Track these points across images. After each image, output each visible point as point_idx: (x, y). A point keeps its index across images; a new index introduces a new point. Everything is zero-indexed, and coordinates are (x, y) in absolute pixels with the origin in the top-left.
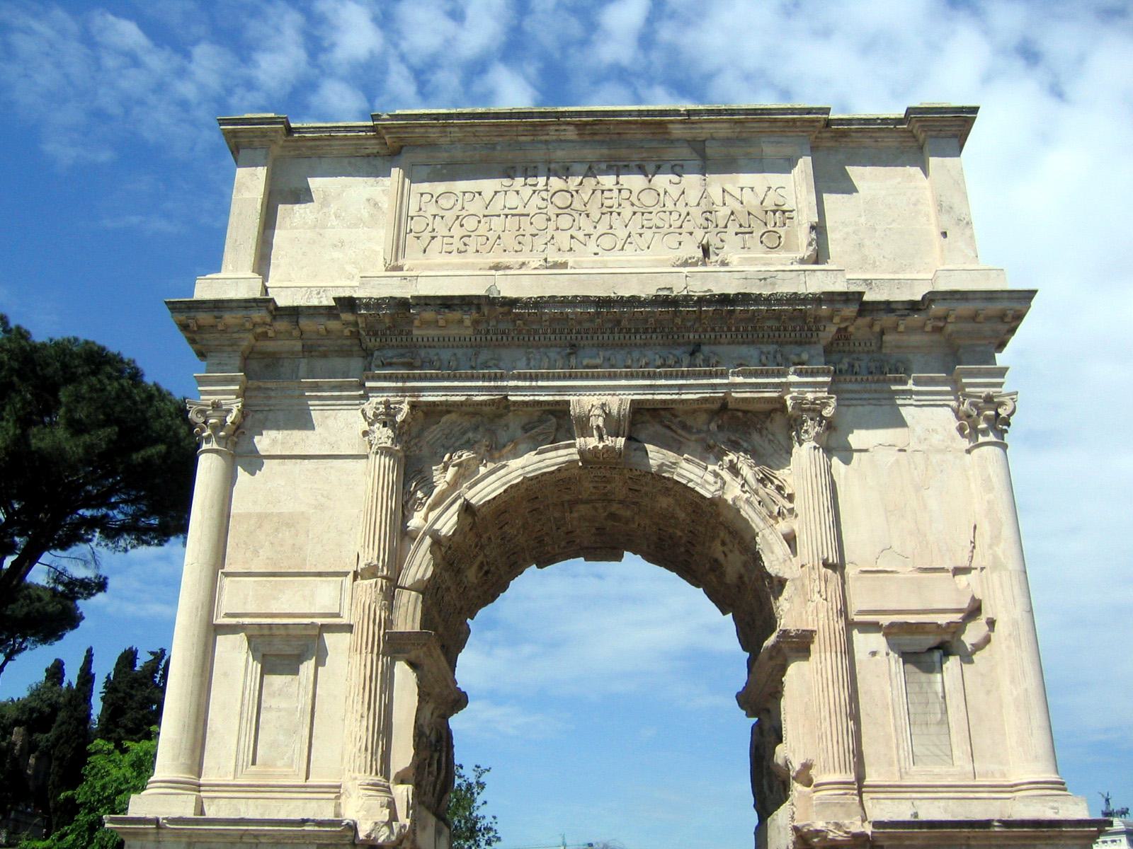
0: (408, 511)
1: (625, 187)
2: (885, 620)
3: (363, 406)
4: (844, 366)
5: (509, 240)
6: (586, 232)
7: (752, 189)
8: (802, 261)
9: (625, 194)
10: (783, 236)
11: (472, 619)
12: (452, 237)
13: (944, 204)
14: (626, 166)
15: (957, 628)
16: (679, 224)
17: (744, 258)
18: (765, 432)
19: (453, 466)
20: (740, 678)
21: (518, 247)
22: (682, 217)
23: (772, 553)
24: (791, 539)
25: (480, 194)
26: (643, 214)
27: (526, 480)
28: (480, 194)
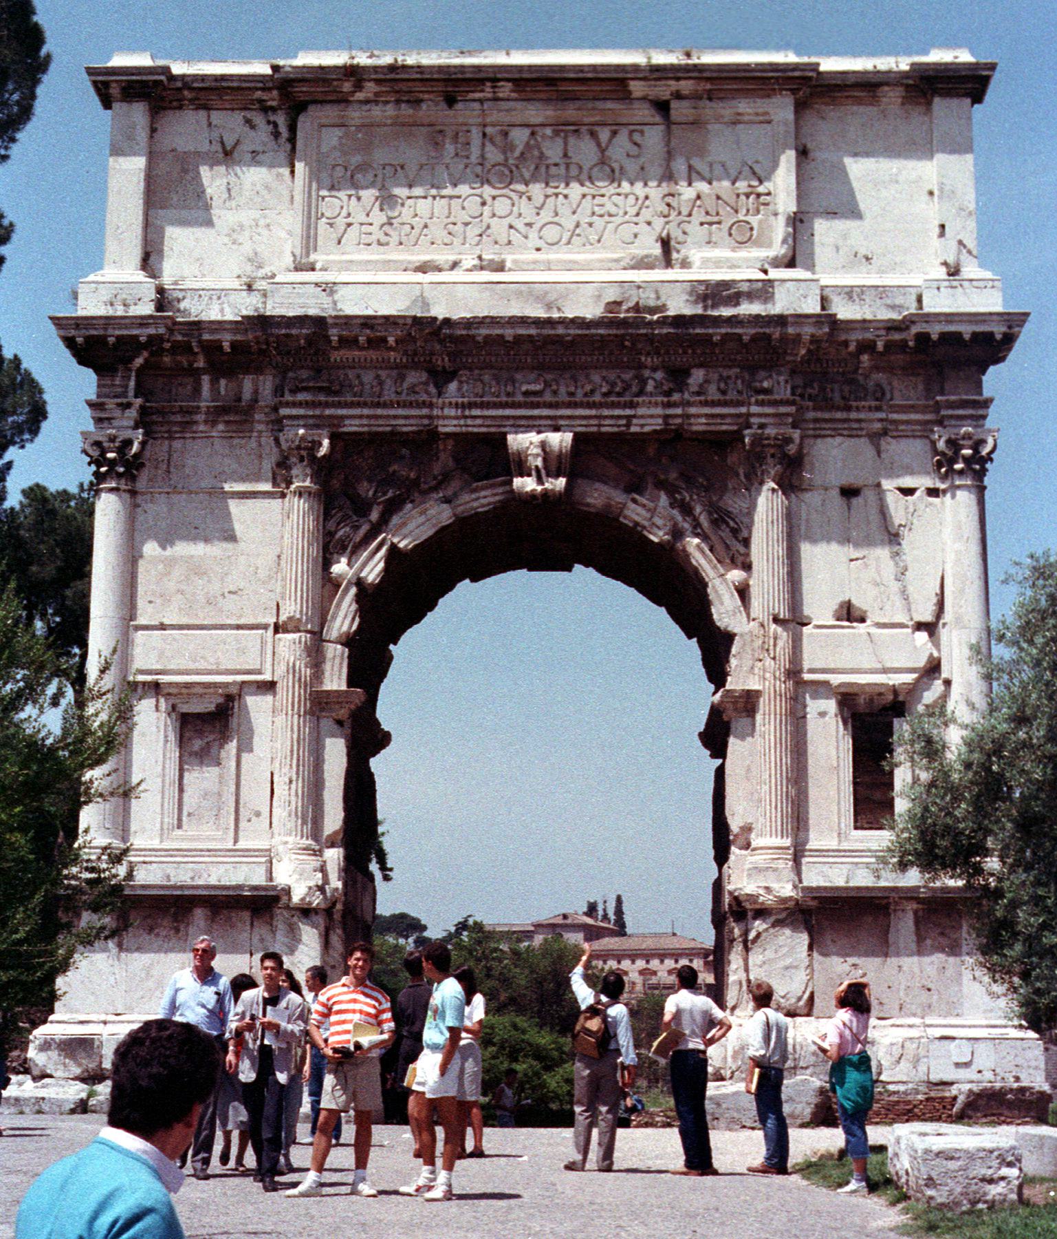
0: (331, 554)
2: (836, 679)
5: (437, 232)
6: (527, 221)
10: (755, 225)
11: (395, 644)
13: (947, 188)
14: (576, 131)
15: (914, 690)
16: (636, 209)
22: (640, 202)
23: (722, 604)
24: (743, 592)
25: (402, 167)
26: (594, 197)
28: (402, 167)
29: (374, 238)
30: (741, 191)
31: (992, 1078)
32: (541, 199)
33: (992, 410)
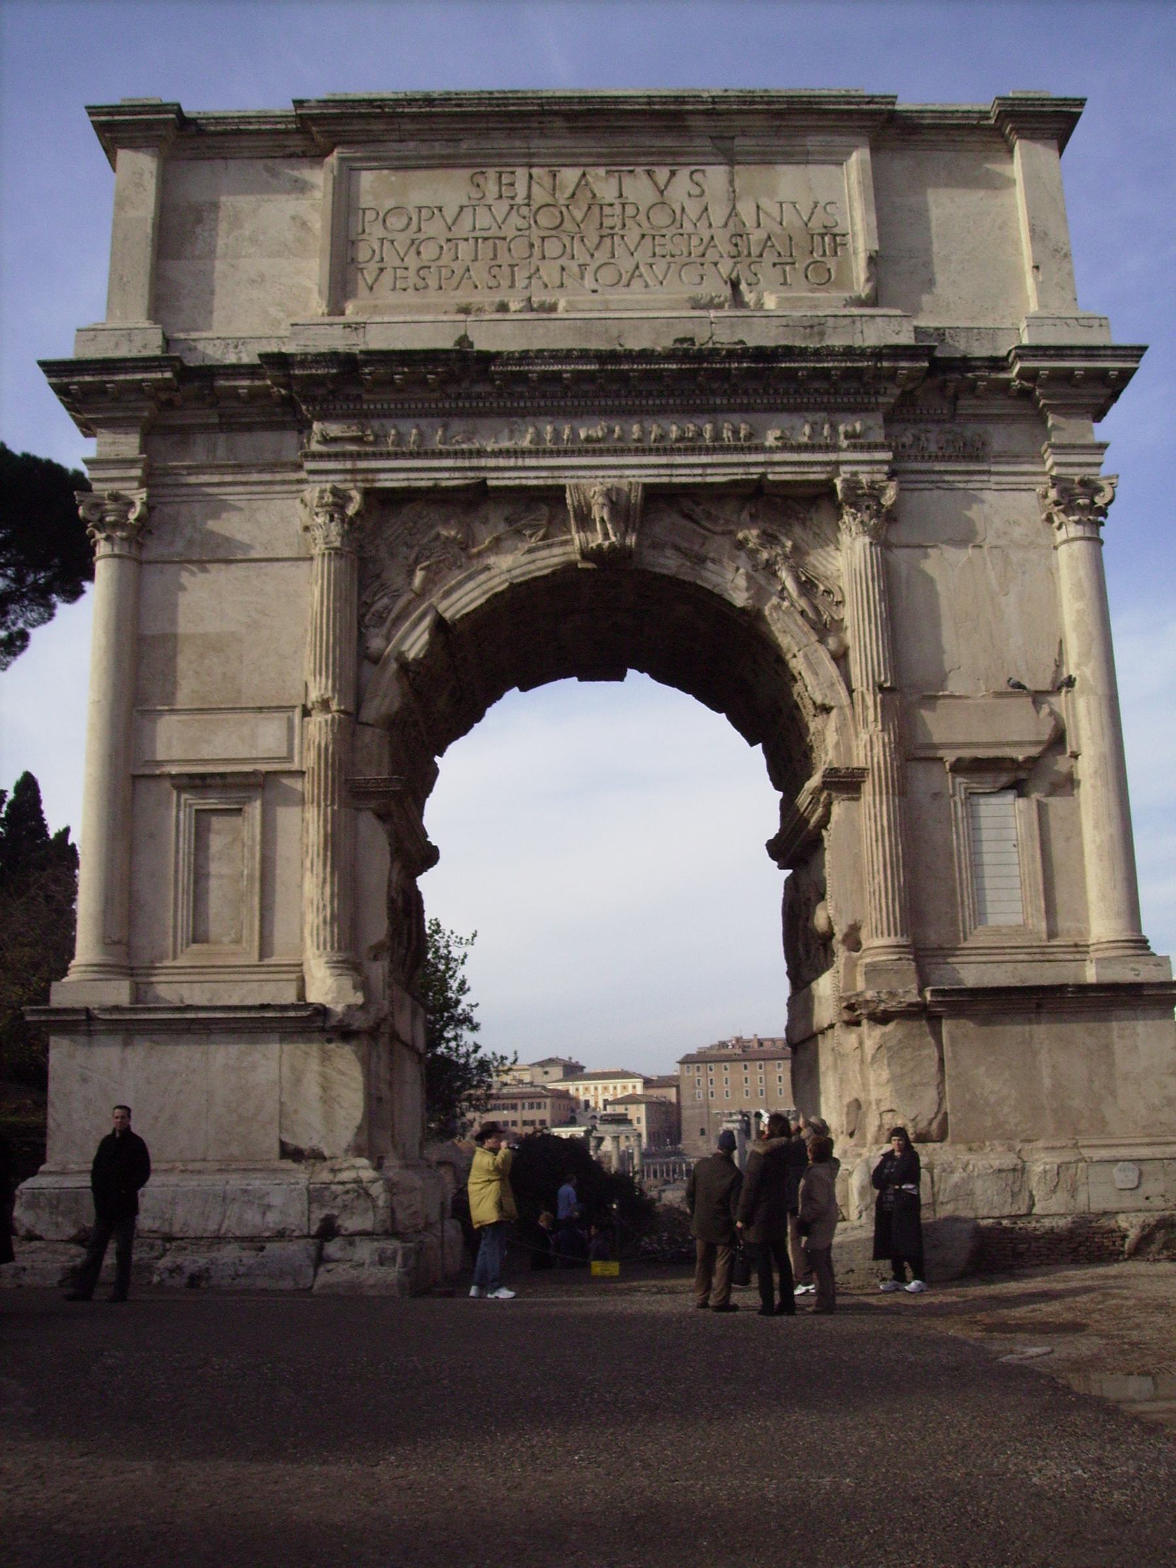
0: (367, 627)
1: (631, 200)
3: (301, 494)
4: (907, 439)
5: (479, 273)
6: (581, 261)
7: (794, 204)
8: (860, 302)
9: (630, 211)
12: (406, 269)
14: (631, 172)
16: (701, 249)
17: (787, 299)
18: (808, 523)
19: (421, 569)
20: (772, 826)
21: (492, 283)
27: (513, 587)
29: (411, 284)
30: (817, 231)
31: (1163, 1205)
32: (596, 240)
33: (1108, 456)
